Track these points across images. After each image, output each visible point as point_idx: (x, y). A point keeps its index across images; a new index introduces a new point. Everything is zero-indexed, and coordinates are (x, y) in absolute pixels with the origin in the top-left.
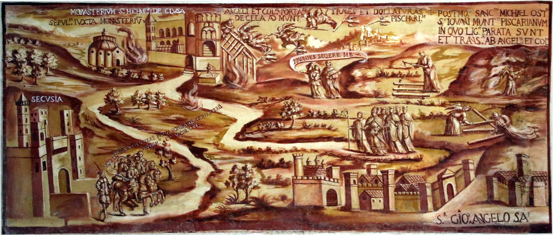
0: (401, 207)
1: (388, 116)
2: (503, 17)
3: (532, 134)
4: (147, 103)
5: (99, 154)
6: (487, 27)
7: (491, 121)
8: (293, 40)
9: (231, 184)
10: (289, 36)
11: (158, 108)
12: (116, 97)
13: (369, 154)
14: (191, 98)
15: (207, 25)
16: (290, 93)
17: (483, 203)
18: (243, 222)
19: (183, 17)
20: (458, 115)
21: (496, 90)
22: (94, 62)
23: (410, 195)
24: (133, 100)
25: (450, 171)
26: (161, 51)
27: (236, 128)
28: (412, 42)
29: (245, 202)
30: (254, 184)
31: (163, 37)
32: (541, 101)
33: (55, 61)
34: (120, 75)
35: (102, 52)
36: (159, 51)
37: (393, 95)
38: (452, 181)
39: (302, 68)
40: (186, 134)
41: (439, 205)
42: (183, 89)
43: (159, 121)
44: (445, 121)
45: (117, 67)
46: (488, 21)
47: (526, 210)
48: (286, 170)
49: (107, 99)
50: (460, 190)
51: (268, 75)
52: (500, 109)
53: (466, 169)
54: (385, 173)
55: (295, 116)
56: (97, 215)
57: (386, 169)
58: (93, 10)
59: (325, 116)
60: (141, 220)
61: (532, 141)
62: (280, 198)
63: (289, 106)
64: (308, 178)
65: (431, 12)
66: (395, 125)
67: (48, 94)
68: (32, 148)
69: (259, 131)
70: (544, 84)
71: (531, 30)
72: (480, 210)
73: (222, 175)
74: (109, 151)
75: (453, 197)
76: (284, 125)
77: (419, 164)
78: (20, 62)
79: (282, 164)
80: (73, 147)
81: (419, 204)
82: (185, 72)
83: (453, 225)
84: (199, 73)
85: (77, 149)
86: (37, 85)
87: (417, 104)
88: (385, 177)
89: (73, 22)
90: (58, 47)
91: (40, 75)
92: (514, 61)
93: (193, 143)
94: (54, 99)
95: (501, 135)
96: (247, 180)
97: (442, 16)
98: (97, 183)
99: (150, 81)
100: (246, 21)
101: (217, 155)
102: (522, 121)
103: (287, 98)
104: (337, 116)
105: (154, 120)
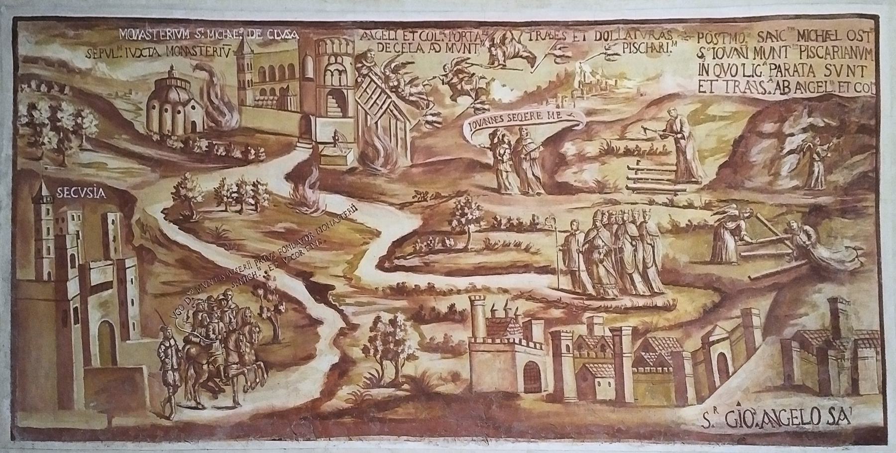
1: (620, 225)
2: (802, 42)
3: (854, 260)
4: (239, 201)
5: (163, 295)
6: (778, 61)
7: (785, 236)
8: (468, 87)
9: (372, 351)
10: (462, 80)
11: (256, 210)
12: (191, 190)
14: (309, 193)
15: (333, 59)
16: (464, 186)
17: (777, 389)
18: (391, 420)
19: (293, 46)
20: (731, 225)
21: (792, 179)
22: (155, 127)
23: (657, 372)
24: (217, 196)
26: (261, 107)
27: (378, 249)
28: (654, 91)
29: (394, 384)
31: (264, 81)
32: (866, 200)
33: (94, 123)
34: (197, 150)
35: (168, 107)
36: (257, 106)
37: (628, 188)
39: (482, 139)
40: (301, 259)
41: (706, 392)
42: (296, 176)
43: (259, 235)
44: (711, 237)
45: (192, 136)
46: (777, 50)
48: (458, 325)
49: (176, 195)
50: (740, 364)
51: (430, 151)
52: (800, 214)
53: (747, 326)
54: (617, 332)
55: (472, 228)
56: (159, 409)
57: (618, 325)
58: (155, 31)
59: (519, 228)
60: (230, 416)
61: (853, 273)
62: (449, 378)
63: (462, 208)
64: (493, 340)
65: (686, 36)
66: (631, 244)
67: (83, 184)
68: (56, 281)
69: (416, 253)
70: (870, 168)
71: (848, 66)
72: (770, 402)
73: (357, 334)
74: (179, 289)
75: (728, 377)
76: (456, 244)
77: (669, 315)
78: (39, 125)
79: (453, 316)
80: (122, 281)
81: (673, 390)
82: (298, 144)
83: (730, 431)
84: (321, 147)
85: (129, 284)
86: (65, 166)
87: (666, 205)
88: (617, 339)
89: (122, 53)
90: (99, 97)
91: (71, 148)
92: (822, 125)
93: (311, 275)
94: (92, 192)
95: (803, 262)
96: (398, 343)
97: (703, 42)
98: (160, 347)
99: (245, 162)
100: (393, 54)
101: (350, 297)
102: (836, 238)
103: (459, 194)
104: (538, 227)
105: (251, 233)
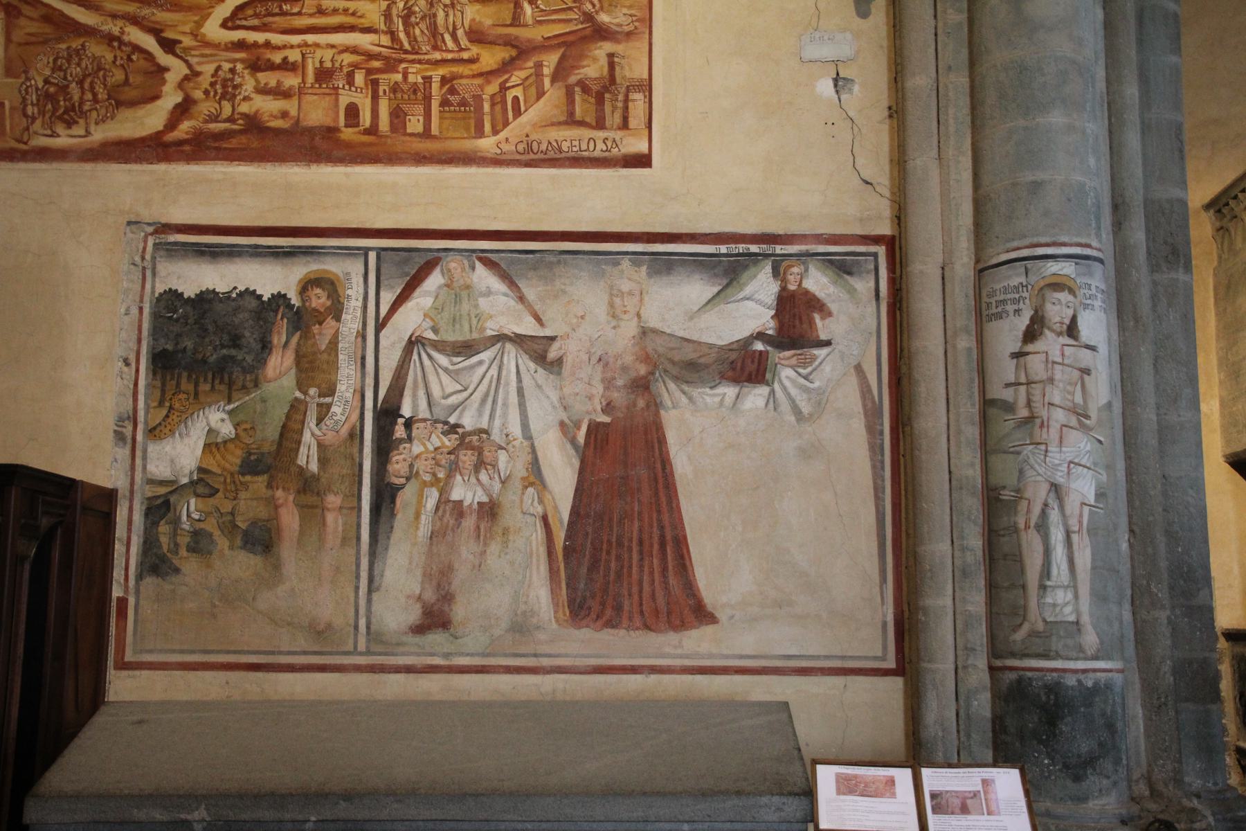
0: (448, 129)
5: (27, 44)
13: (406, 52)
17: (560, 124)
25: (517, 77)
29: (230, 120)
30: (244, 93)
38: (518, 92)
40: (153, 18)
47: (618, 135)
53: (539, 75)
54: (427, 80)
57: (429, 74)
61: (629, 35)
69: (256, 15)
73: (200, 79)
77: (474, 67)
79: (286, 66)
83: (518, 157)
93: (162, 31)
96: (235, 87)
